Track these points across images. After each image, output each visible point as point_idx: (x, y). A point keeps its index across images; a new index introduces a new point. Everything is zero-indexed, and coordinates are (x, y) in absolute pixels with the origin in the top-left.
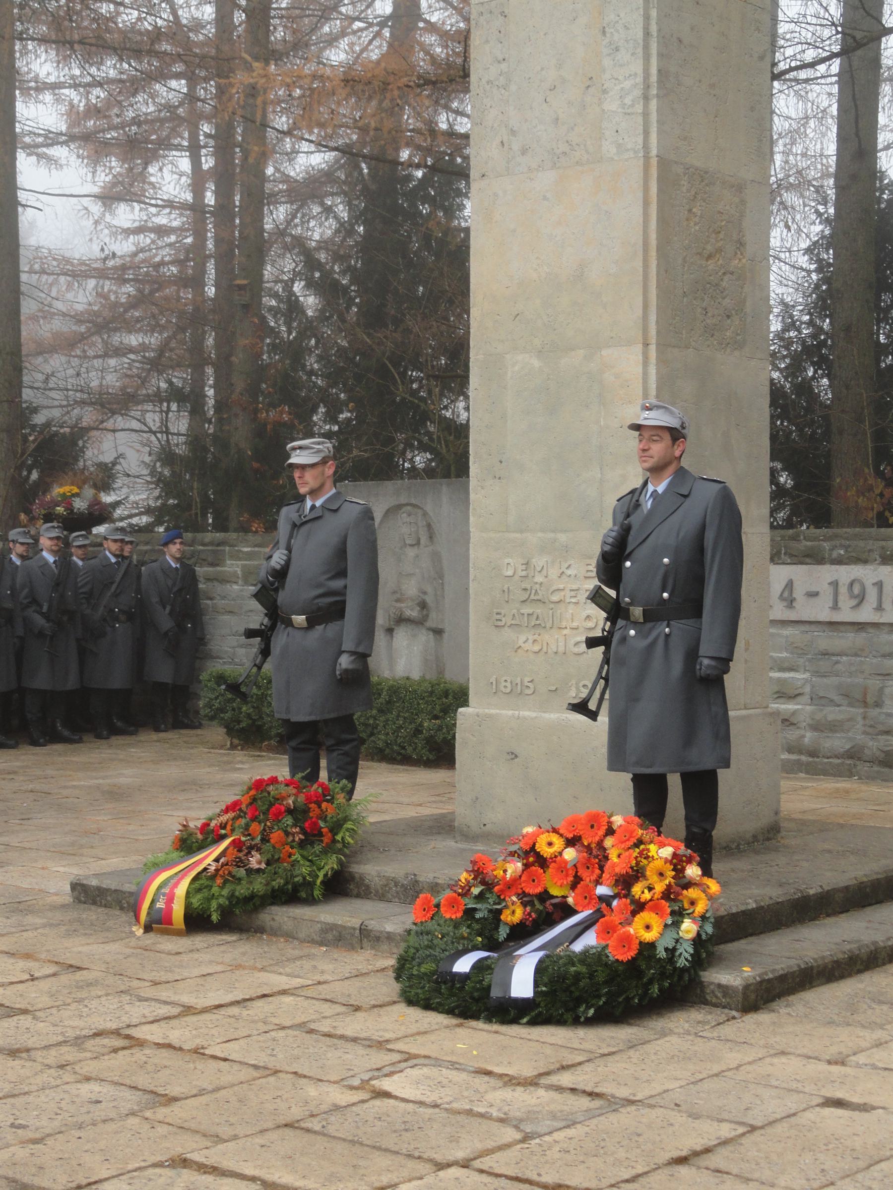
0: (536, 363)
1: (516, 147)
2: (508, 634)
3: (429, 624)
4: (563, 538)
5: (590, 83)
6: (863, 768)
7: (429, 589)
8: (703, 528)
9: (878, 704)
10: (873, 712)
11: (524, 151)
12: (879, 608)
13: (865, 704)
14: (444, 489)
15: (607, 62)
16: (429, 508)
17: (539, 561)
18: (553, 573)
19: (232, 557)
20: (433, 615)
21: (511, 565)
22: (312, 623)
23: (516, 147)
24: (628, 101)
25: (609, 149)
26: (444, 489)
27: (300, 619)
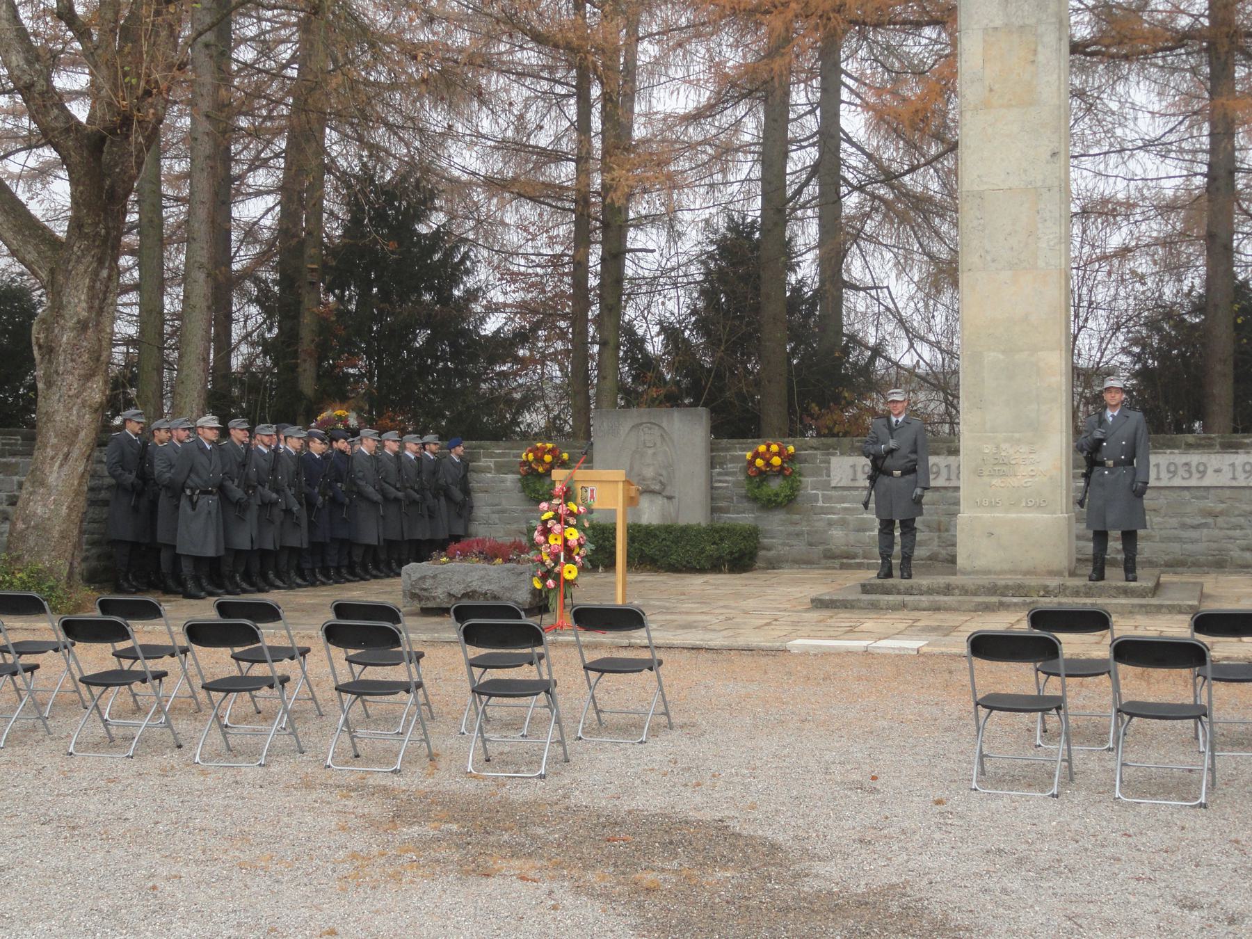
0: (1001, 357)
1: (989, 258)
2: (986, 479)
3: (666, 493)
4: (1017, 435)
5: (1031, 234)
6: (939, 565)
7: (664, 473)
8: (1137, 429)
9: (947, 530)
10: (945, 535)
11: (993, 261)
12: (949, 479)
13: (939, 530)
14: (676, 414)
15: (1040, 225)
16: (664, 425)
17: (1004, 446)
18: (1011, 451)
19: (485, 456)
20: (668, 488)
21: (988, 449)
22: (903, 474)
23: (989, 258)
24: (1052, 243)
25: (1041, 263)
26: (676, 414)
27: (897, 473)
